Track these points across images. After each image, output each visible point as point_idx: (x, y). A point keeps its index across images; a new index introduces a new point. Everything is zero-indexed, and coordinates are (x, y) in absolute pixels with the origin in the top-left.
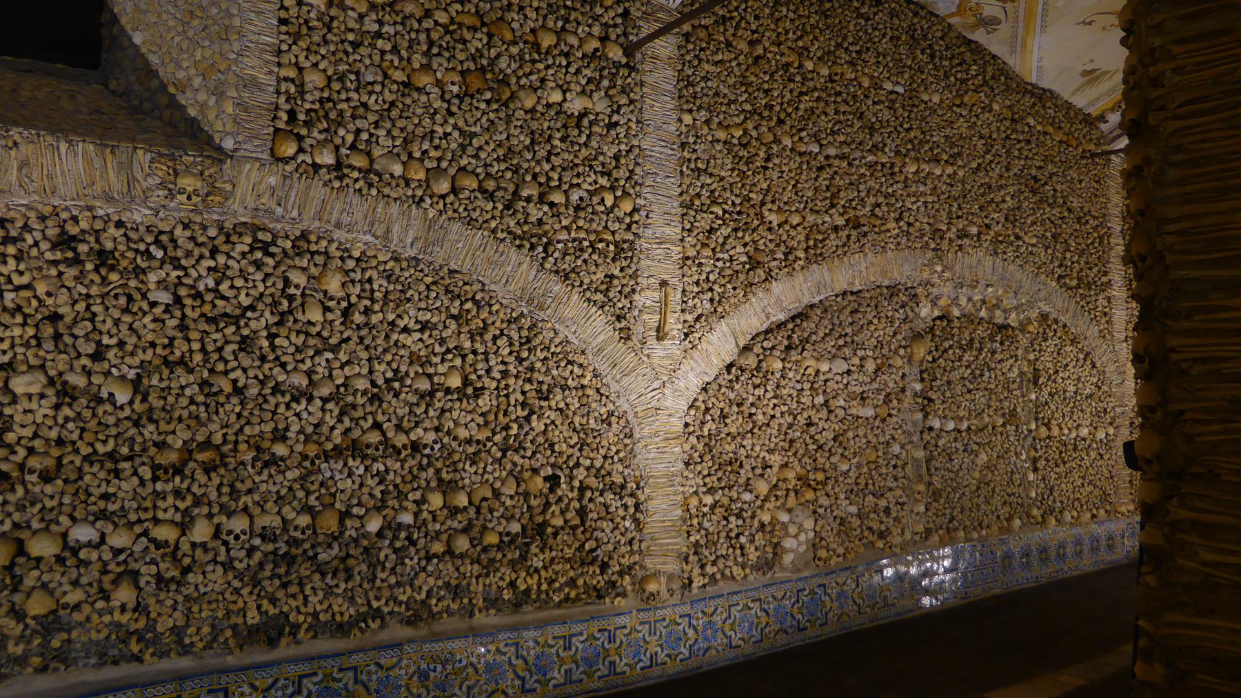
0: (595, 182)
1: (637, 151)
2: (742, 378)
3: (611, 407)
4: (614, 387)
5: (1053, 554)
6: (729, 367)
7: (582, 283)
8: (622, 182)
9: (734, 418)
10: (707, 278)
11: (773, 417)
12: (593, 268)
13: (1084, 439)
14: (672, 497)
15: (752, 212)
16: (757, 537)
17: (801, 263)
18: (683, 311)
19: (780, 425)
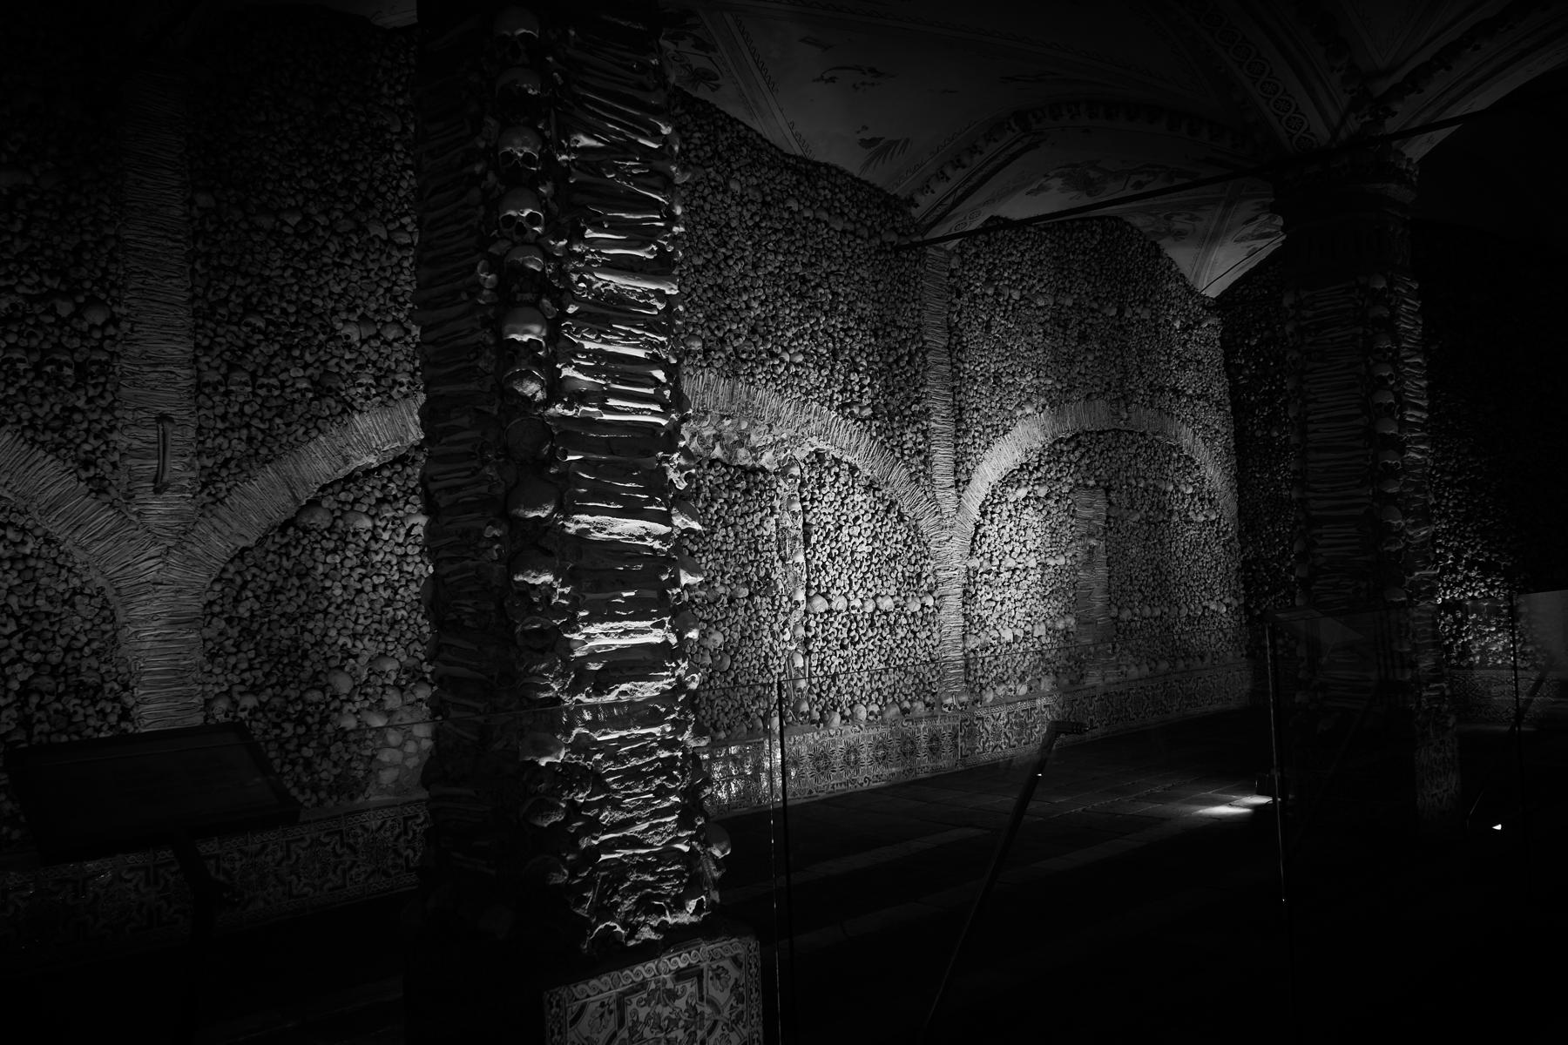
0: (40, 284)
1: (112, 243)
2: (305, 542)
3: (76, 582)
4: (79, 556)
5: (838, 761)
6: (283, 528)
7: (19, 421)
8: (88, 285)
9: (293, 593)
10: (241, 410)
11: (360, 591)
12: (36, 399)
13: (886, 613)
14: (182, 700)
15: (315, 324)
16: (333, 749)
17: (404, 389)
18: (199, 454)
19: (372, 602)
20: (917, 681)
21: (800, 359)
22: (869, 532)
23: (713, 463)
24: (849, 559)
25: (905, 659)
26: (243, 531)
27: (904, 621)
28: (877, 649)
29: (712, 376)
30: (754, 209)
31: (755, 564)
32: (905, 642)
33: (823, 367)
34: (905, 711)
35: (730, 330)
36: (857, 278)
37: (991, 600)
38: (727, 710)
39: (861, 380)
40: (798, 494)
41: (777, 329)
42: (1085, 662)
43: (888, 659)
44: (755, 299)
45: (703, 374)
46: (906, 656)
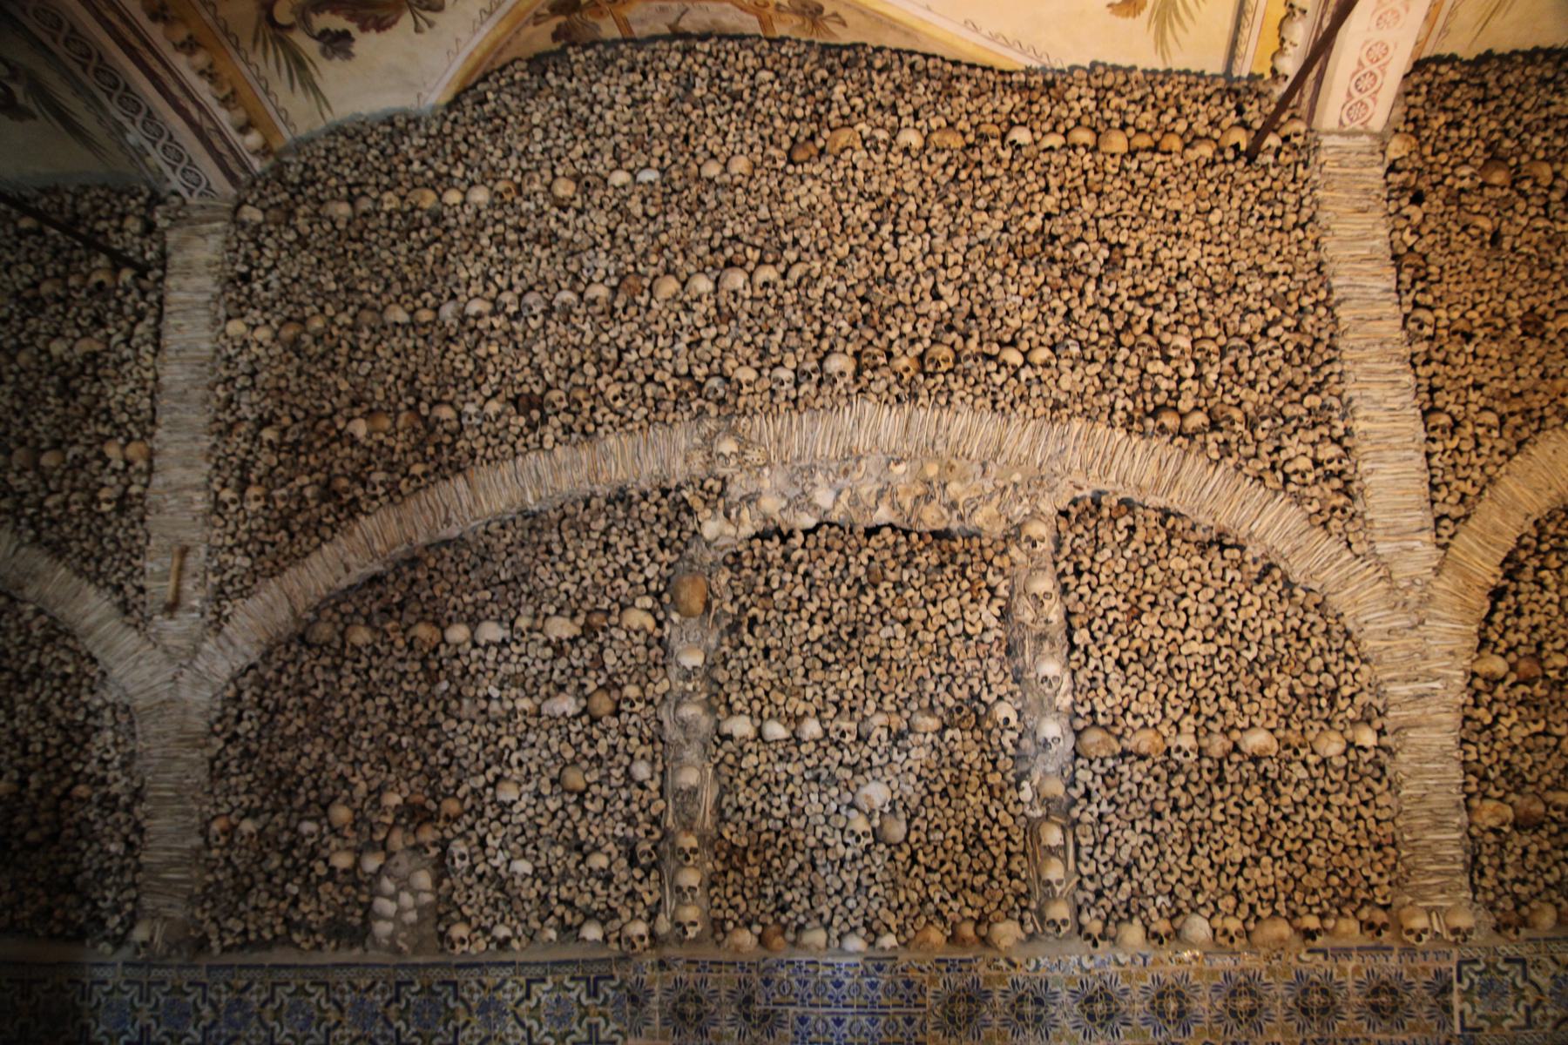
20: (1335, 880)
21: (1041, 355)
22: (1205, 620)
23: (872, 532)
24: (1161, 666)
25: (1305, 842)
26: (246, 648)
27: (1302, 773)
28: (1237, 822)
29: (869, 406)
30: (943, 158)
31: (946, 680)
32: (1302, 809)
33: (1093, 360)
34: (1310, 934)
35: (902, 335)
36: (1159, 214)
37: (1546, 733)
38: (895, 904)
39: (1177, 370)
40: (1051, 567)
41: (990, 319)
43: (1262, 839)
44: (948, 280)
45: (850, 403)
46: (1308, 835)
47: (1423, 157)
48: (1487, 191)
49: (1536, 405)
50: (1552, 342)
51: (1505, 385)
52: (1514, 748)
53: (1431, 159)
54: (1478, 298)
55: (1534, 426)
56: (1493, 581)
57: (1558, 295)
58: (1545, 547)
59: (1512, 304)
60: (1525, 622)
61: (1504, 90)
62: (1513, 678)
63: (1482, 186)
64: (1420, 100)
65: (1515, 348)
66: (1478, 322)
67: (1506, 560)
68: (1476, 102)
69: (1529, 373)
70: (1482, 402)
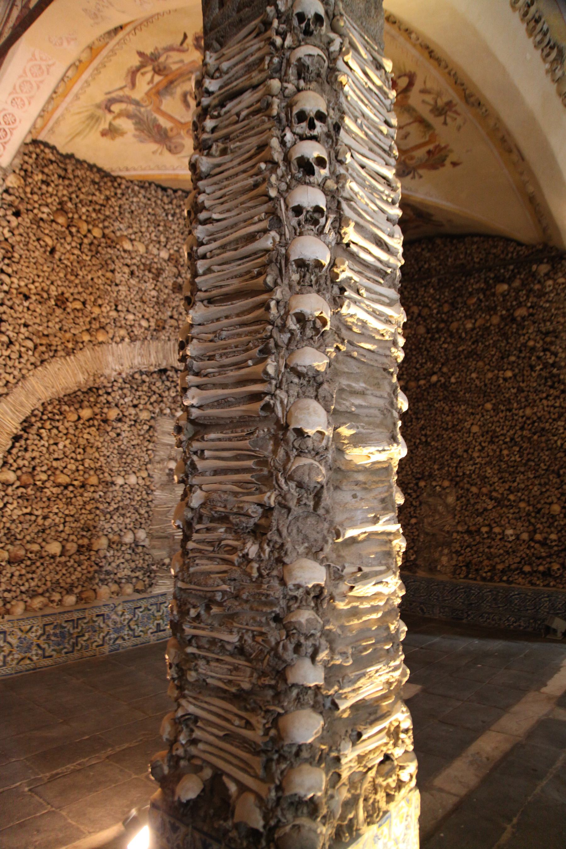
37: (31, 514)
42: (155, 572)
47: (25, 193)
48: (54, 225)
49: (54, 343)
50: (69, 313)
51: (41, 328)
52: (13, 521)
53: (29, 196)
54: (36, 279)
55: (51, 354)
56: (15, 431)
57: (76, 291)
58: (45, 417)
59: (53, 288)
60: (28, 455)
61: (75, 177)
62: (18, 484)
63: (53, 221)
64: (31, 161)
65: (50, 311)
66: (34, 291)
67: (25, 421)
68: (60, 176)
69: (54, 326)
70: (27, 334)
